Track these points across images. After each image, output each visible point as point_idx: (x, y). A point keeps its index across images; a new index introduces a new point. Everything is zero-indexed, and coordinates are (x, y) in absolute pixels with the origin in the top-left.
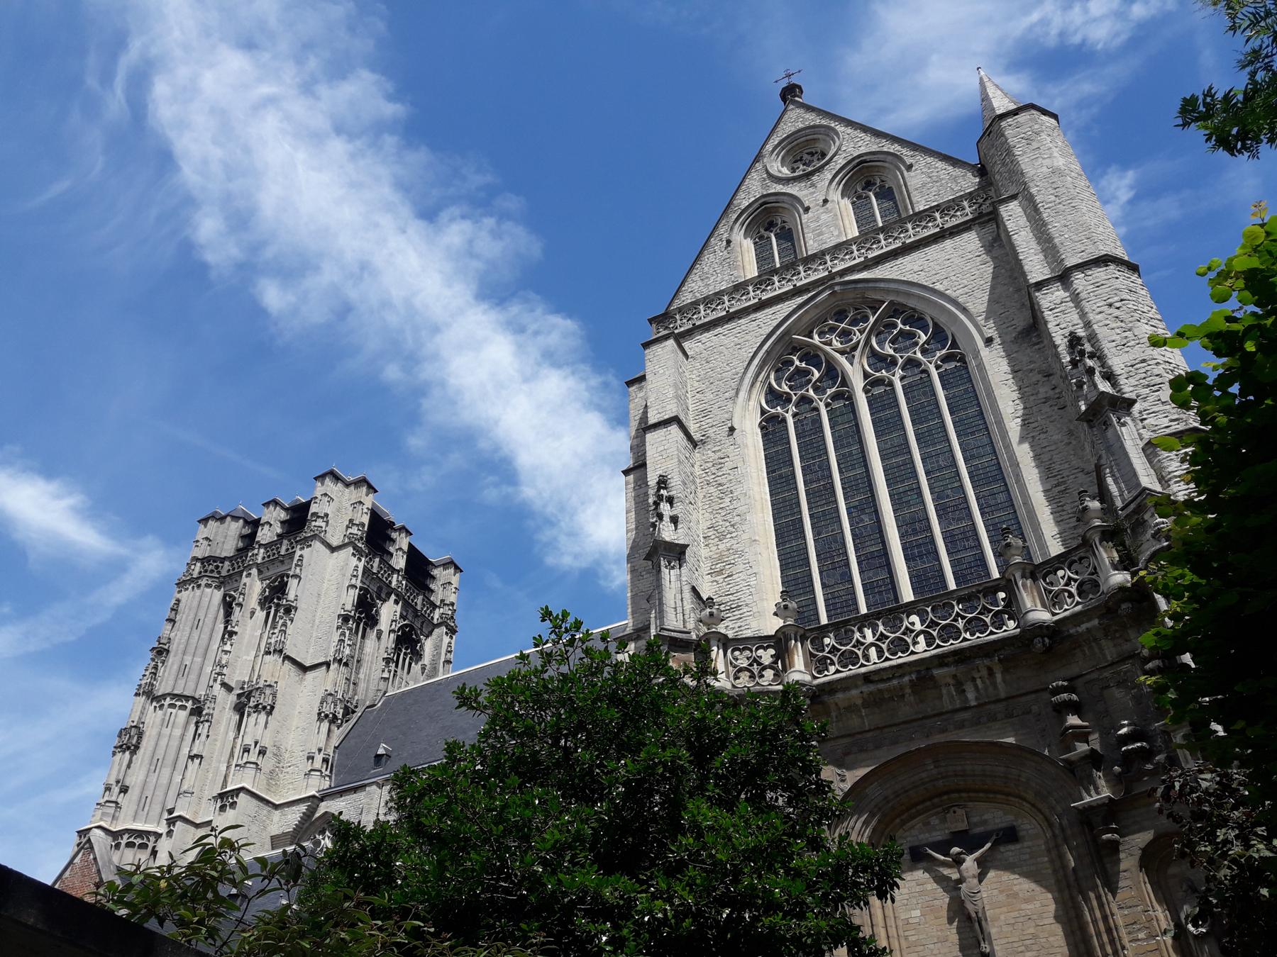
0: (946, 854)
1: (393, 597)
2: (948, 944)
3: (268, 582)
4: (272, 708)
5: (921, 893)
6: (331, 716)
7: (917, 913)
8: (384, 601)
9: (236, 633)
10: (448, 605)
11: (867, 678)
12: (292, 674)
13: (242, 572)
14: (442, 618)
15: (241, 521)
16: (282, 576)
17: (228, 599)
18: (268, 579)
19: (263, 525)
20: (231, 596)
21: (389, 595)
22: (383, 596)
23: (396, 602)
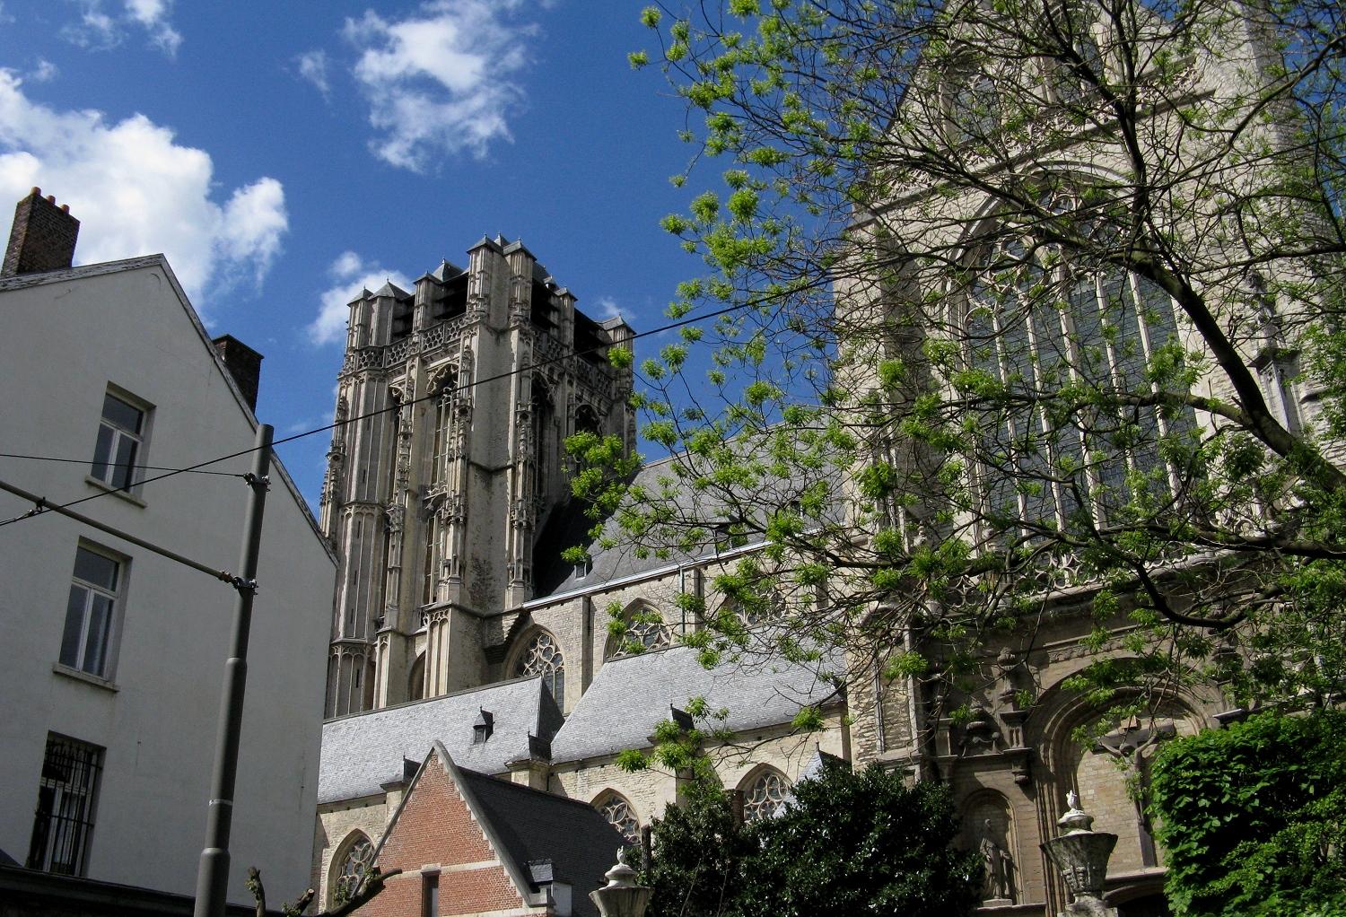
0: (1117, 748)
1: (567, 378)
2: (1114, 816)
3: (433, 374)
4: (465, 519)
5: (1098, 777)
6: (524, 524)
7: (1091, 792)
8: (557, 383)
9: (411, 435)
10: (625, 377)
11: (1059, 602)
12: (479, 481)
13: (405, 363)
14: (620, 392)
15: (393, 301)
16: (448, 367)
17: (394, 394)
18: (434, 371)
19: (418, 307)
20: (396, 390)
21: (561, 375)
22: (555, 378)
23: (570, 383)
